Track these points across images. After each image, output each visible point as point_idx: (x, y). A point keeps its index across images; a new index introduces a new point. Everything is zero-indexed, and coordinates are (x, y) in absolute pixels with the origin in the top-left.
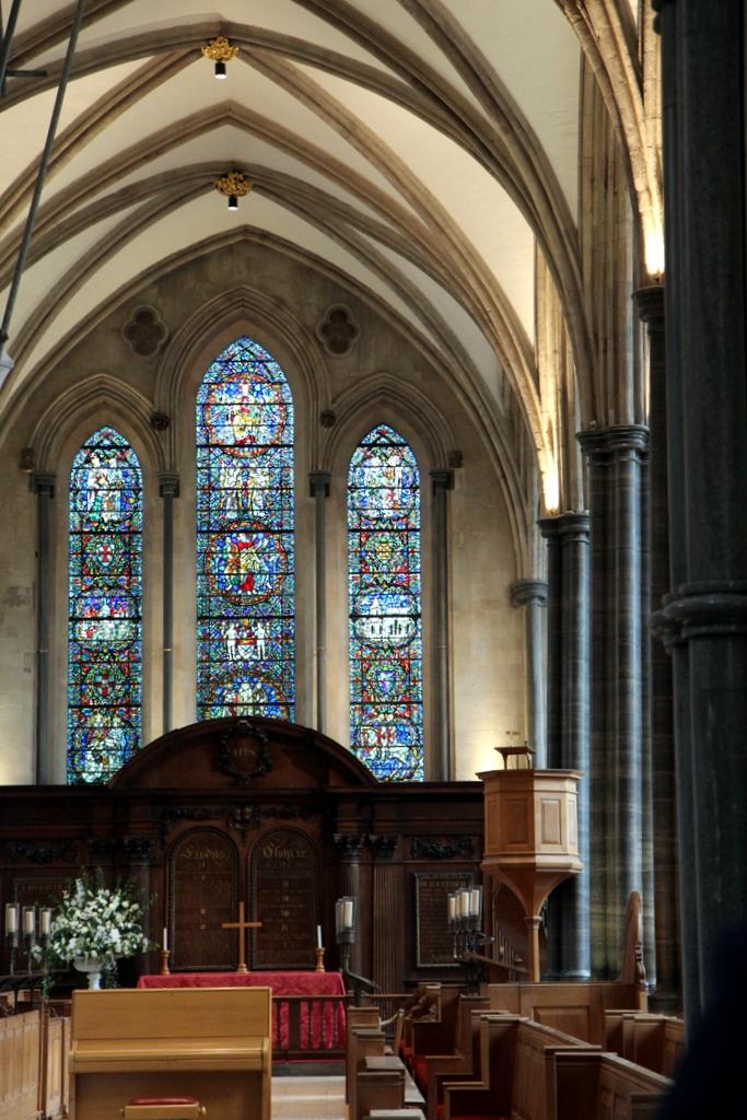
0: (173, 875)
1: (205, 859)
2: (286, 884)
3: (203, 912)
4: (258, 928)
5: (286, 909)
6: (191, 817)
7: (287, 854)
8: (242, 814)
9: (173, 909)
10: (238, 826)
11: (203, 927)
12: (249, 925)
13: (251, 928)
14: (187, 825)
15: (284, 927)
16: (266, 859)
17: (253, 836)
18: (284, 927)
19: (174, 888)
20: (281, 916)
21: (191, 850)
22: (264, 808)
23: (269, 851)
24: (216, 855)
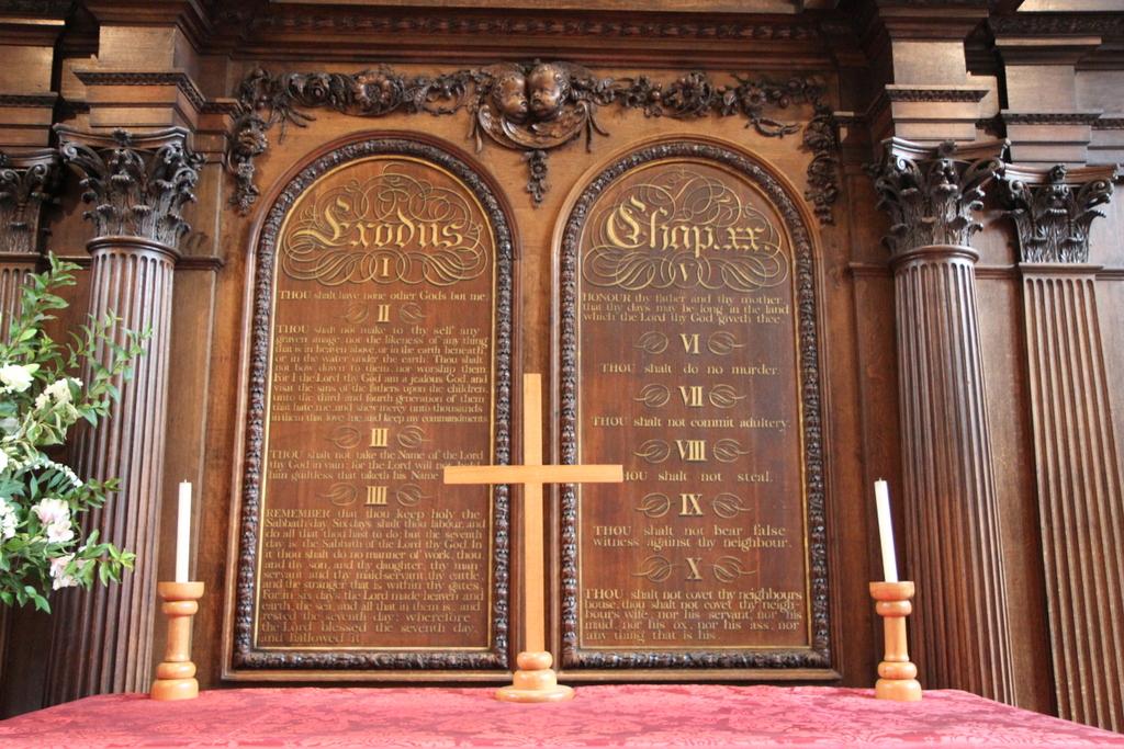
0: (272, 301)
1: (392, 251)
2: (692, 344)
3: (379, 437)
4: (604, 501)
5: (695, 434)
6: (340, 99)
7: (692, 237)
8: (528, 91)
9: (264, 431)
10: (510, 130)
11: (377, 495)
12: (556, 474)
13: (563, 489)
14: (329, 127)
15: (690, 503)
16: (622, 253)
17: (569, 171)
18: (690, 503)
19: (270, 345)
20: (676, 463)
21: (340, 215)
22: (606, 79)
23: (627, 225)
24: (431, 235)
